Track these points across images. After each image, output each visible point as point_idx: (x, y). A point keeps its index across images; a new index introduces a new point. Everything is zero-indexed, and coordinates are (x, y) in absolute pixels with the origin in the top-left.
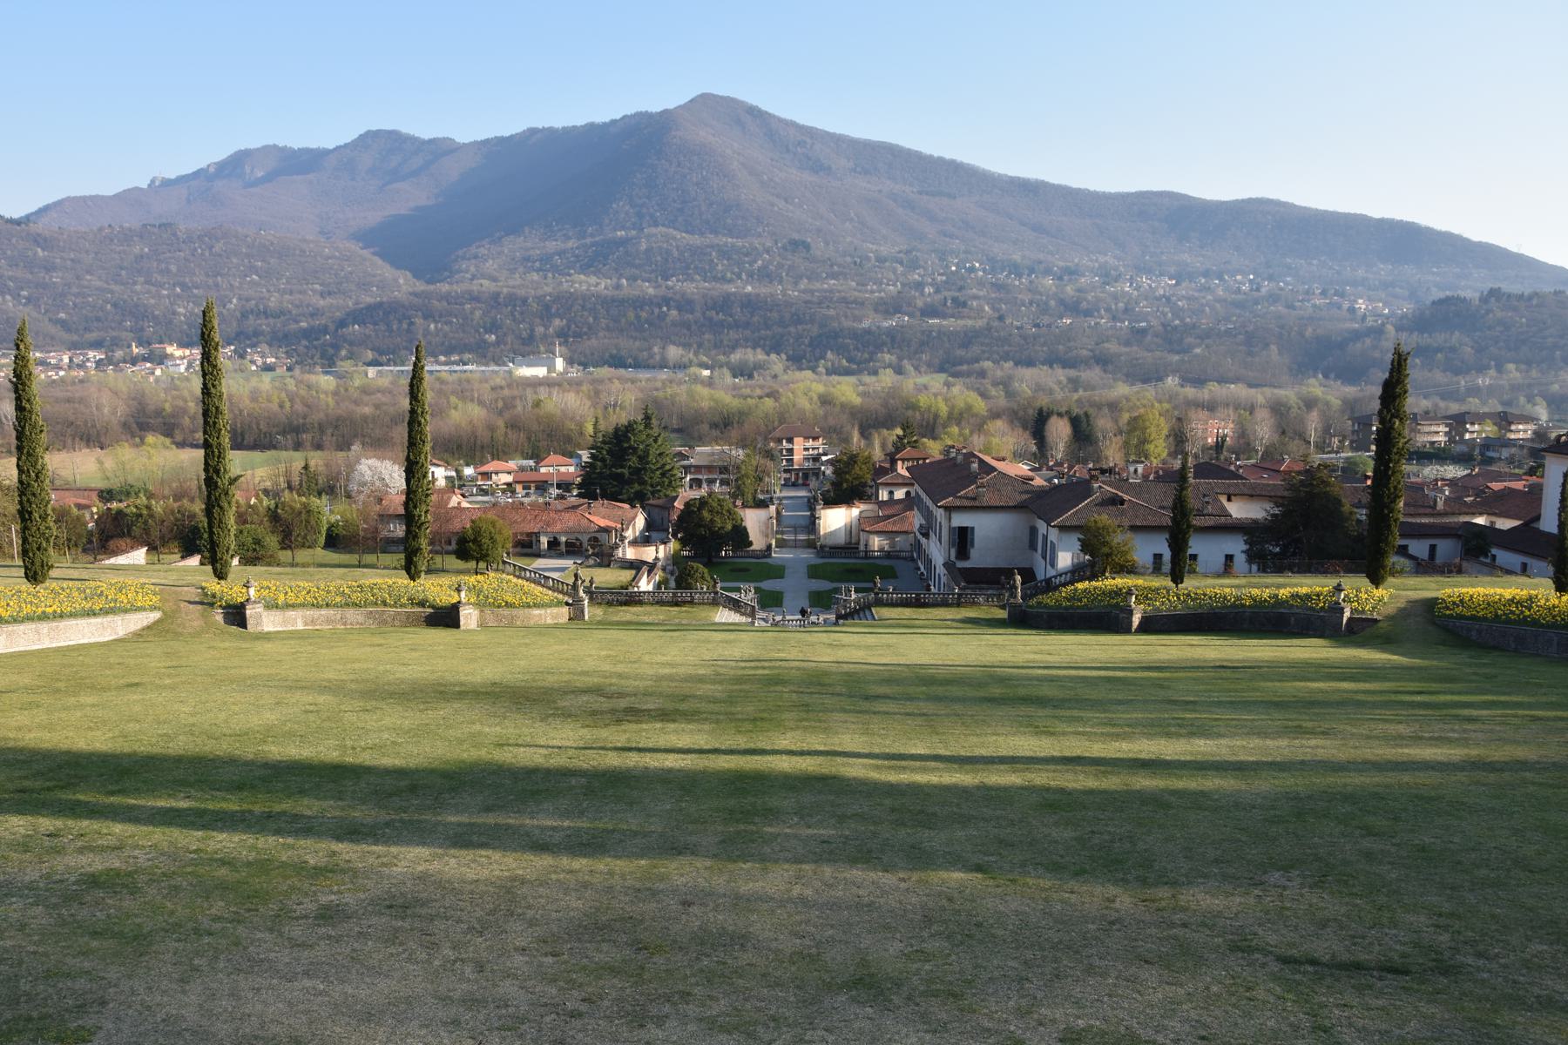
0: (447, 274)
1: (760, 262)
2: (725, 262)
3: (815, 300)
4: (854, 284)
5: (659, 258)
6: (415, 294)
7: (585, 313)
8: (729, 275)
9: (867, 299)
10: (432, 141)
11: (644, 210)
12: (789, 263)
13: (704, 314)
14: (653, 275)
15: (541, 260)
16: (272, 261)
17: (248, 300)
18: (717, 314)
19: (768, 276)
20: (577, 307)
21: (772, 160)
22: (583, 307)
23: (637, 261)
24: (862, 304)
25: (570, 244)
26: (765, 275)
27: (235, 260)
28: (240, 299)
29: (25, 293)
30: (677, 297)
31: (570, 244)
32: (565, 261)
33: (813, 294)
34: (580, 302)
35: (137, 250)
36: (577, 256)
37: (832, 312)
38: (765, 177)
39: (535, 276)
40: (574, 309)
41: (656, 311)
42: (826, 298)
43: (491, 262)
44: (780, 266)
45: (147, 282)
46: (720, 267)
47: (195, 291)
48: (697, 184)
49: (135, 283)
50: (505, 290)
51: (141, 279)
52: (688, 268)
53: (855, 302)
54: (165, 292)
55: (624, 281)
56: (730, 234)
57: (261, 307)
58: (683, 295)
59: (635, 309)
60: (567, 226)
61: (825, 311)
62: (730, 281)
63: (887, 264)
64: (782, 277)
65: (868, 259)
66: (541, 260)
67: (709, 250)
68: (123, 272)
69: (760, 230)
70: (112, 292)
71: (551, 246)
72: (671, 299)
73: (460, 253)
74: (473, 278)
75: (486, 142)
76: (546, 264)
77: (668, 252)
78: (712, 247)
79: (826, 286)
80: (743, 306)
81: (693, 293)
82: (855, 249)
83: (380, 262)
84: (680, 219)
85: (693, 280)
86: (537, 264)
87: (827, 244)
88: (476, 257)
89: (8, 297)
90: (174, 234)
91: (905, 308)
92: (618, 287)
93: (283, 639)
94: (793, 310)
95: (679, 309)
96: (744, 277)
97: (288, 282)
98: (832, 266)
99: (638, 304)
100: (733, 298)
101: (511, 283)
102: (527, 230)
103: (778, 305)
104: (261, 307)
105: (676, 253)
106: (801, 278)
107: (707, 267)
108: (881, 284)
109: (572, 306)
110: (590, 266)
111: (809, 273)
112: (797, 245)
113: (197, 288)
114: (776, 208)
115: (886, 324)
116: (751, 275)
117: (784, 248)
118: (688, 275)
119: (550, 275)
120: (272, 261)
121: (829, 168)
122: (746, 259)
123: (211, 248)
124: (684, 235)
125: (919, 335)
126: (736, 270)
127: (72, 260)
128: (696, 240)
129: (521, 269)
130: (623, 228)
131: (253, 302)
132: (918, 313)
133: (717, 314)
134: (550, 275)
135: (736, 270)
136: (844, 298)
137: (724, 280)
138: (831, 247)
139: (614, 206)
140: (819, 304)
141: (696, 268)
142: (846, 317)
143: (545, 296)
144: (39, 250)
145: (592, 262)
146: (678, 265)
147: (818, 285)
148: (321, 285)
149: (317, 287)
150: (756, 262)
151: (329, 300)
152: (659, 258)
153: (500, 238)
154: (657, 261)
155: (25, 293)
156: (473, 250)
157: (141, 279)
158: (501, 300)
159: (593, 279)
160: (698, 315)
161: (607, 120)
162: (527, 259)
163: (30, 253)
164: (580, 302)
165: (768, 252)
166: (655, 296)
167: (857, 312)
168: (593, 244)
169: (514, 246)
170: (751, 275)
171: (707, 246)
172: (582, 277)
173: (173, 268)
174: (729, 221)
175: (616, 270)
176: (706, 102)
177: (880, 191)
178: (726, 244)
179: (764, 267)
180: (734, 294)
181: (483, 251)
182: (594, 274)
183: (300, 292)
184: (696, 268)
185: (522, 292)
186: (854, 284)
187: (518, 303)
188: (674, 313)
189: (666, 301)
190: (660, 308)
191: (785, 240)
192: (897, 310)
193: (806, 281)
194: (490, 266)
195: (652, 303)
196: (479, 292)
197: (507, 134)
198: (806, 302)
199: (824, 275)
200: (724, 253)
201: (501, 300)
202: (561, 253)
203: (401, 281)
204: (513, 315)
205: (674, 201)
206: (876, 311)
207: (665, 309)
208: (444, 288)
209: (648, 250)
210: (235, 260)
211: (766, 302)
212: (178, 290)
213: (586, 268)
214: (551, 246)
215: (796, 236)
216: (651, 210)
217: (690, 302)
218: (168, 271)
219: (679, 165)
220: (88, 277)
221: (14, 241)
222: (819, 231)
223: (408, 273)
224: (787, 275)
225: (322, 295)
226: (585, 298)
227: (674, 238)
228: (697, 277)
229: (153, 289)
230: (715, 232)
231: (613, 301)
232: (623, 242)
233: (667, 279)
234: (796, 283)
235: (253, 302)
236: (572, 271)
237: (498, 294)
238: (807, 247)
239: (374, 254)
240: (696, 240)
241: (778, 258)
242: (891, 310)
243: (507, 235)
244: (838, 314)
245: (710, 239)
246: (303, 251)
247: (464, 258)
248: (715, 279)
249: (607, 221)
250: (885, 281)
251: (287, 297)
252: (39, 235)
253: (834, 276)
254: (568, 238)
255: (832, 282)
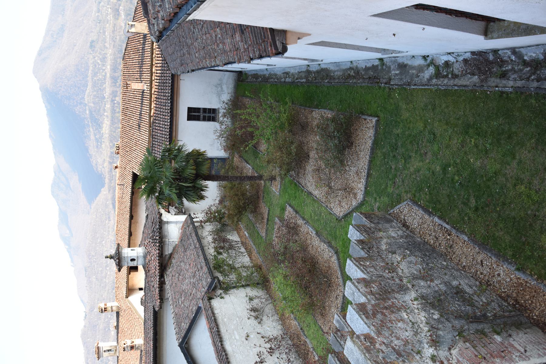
0: (102, 176)
1: (99, 61)
2: (98, 74)
3: (113, 43)
4: (108, 25)
5: (97, 100)
6: (109, 191)
7: (117, 131)
8: (103, 74)
9: (113, 23)
10: (55, 173)
11: (79, 101)
12: (99, 50)
13: (118, 87)
14: (103, 103)
15: (98, 142)
16: (98, 236)
17: (111, 246)
18: (118, 82)
19: (104, 58)
20: (114, 134)
21: (59, 48)
22: (114, 132)
23: (98, 108)
24: (115, 24)
25: (91, 130)
26: (104, 59)
27: (98, 248)
28: (111, 249)
29: (109, 316)
30: (111, 96)
31: (91, 130)
32: (98, 134)
33: (111, 44)
34: (112, 133)
35: (94, 280)
36: (96, 129)
37: (118, 37)
38: (66, 53)
39: (103, 146)
40: (115, 135)
41: (116, 105)
42: (112, 39)
43: (98, 160)
44: (100, 53)
45: (105, 278)
46: (100, 77)
47: (108, 263)
48: (68, 80)
49: (105, 282)
50: (108, 159)
51: (104, 280)
52: (100, 89)
53: (114, 27)
54: (109, 273)
55: (105, 114)
56: (88, 70)
57: (114, 242)
58: (110, 94)
59: (115, 113)
60: (85, 131)
61: (118, 40)
62: (106, 73)
63: (100, 8)
64: (105, 53)
65: (98, 16)
66: (98, 142)
67: (94, 80)
68: (102, 285)
69: (86, 58)
70: (109, 290)
71: (92, 137)
72: (112, 99)
73: (95, 169)
74: (103, 167)
75: (54, 153)
76: (99, 141)
77: (95, 96)
78: (92, 79)
79: (108, 36)
80: (115, 72)
81: (110, 90)
82: (94, 21)
83: (98, 198)
84: (82, 88)
85: (105, 88)
86: (99, 144)
87: (92, 32)
88: (96, 164)
89: (111, 321)
90: (89, 267)
91: (117, 7)
92: (107, 116)
93: (221, 341)
94: (117, 53)
95: (115, 96)
96: (104, 68)
97: (105, 231)
98: (100, 33)
99: (113, 112)
100: (112, 75)
101: (106, 155)
102: (86, 145)
103: (115, 58)
104: (114, 242)
105: (95, 93)
106: (105, 46)
107: (100, 82)
108: (107, 13)
109: (114, 136)
110: (100, 125)
111: (103, 42)
112: (92, 45)
113: (107, 262)
114: (78, 51)
115: (123, 17)
116: (104, 65)
117: (93, 51)
118: (103, 89)
119: (103, 140)
120: (98, 236)
121: (62, 25)
122: (97, 66)
123: (93, 256)
124: (88, 89)
125: (127, 4)
126: (101, 71)
127: (98, 301)
128: (90, 84)
129: (101, 150)
130: (85, 110)
131: (112, 245)
132: (119, 2)
133: (118, 82)
134: (103, 140)
135: (101, 71)
136: (113, 31)
137: (105, 76)
138: (93, 30)
139: (77, 112)
140: (114, 41)
141: (100, 86)
142: (120, 32)
143: (110, 145)
144: (95, 310)
145: (98, 125)
146: (99, 93)
147: (108, 40)
148: (106, 220)
149: (107, 222)
150: (98, 63)
151: (112, 219)
152: (97, 100)
153: (90, 155)
154: (98, 101)
155: (109, 316)
156: (94, 165)
157: (104, 280)
158: (111, 161)
159: (104, 125)
160: (118, 89)
161: (45, 109)
162: (97, 147)
163: (96, 313)
164: (112, 133)
165: (94, 57)
166: (111, 105)
167: (118, 27)
168: (92, 123)
169: (92, 150)
170: (104, 65)
171: (92, 81)
172: (103, 129)
173: (100, 269)
174: (83, 70)
175: (101, 116)
176: (36, 72)
177: (71, 6)
178: (92, 73)
179: (100, 59)
180: (110, 74)
181: (94, 162)
182: (102, 124)
183: (109, 228)
184: (100, 86)
185: (109, 154)
186: (108, 25)
187: (112, 155)
188: (117, 99)
189: (112, 101)
190: (115, 103)
191: (90, 50)
192: (117, 10)
193: (106, 44)
194: (100, 161)
195: (113, 106)
196: (108, 169)
197: (52, 146)
198: (114, 47)
199: (104, 36)
200: (95, 74)
201: (111, 161)
202: (95, 135)
203: (105, 193)
204: (117, 158)
205: (75, 90)
206: (118, 19)
207: (115, 102)
208: (107, 181)
209: (94, 103)
210: (98, 248)
211: (113, 63)
212: (108, 268)
213: (101, 128)
214: (92, 137)
215: (89, 44)
216: (79, 99)
217: (113, 92)
218: (101, 271)
219: (61, 87)
220: (104, 296)
221: (92, 318)
222: (87, 34)
223: (102, 190)
224: (104, 51)
225: (110, 220)
226: (111, 131)
227: (89, 93)
228: (104, 86)
229: (107, 276)
230: (87, 76)
231: (112, 120)
232: (91, 112)
233: (104, 98)
234: (107, 48)
235: (112, 245)
236: (102, 132)
237: (109, 162)
238: (93, 42)
239: (96, 199)
240: (90, 84)
241: (97, 54)
242: (118, 13)
243: (88, 152)
244: (119, 35)
245: (89, 79)
246: (94, 225)
247: (97, 169)
248: (105, 79)
249: (83, 116)
250: (106, 12)
251: (110, 233)
252: (90, 310)
253: (104, 32)
254: (89, 131)
255: (106, 33)
